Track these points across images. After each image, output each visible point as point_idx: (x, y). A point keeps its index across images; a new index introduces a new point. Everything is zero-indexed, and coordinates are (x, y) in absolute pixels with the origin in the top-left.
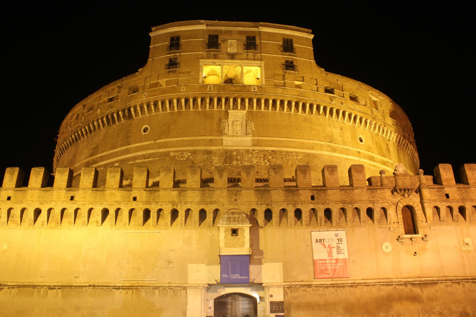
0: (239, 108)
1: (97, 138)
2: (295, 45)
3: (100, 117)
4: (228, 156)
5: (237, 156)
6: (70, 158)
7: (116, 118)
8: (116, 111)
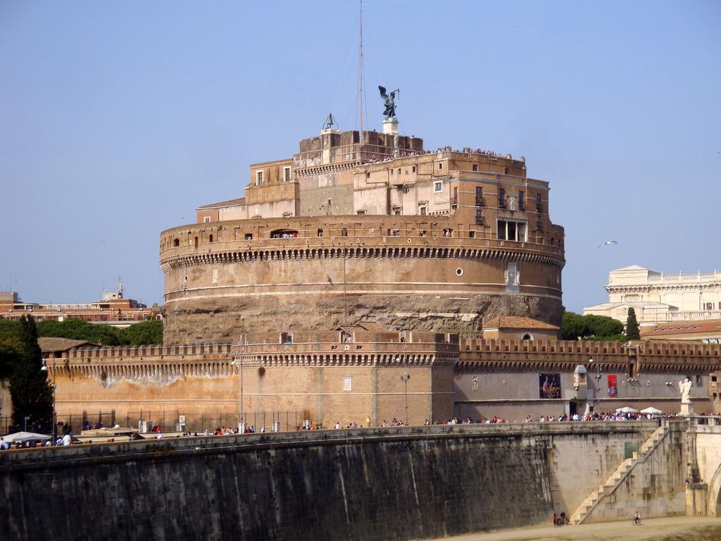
1: (405, 265)
2: (542, 200)
3: (413, 248)
4: (509, 301)
6: (361, 272)
8: (432, 248)
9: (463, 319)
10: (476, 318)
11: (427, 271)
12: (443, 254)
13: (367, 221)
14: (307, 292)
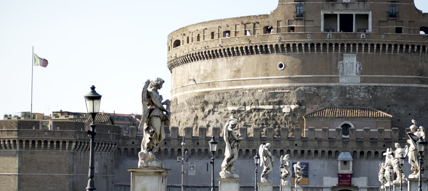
0: (351, 51)
1: (237, 63)
3: (239, 47)
4: (343, 91)
5: (349, 91)
6: (209, 71)
7: (254, 51)
8: (254, 45)
9: (284, 110)
10: (295, 109)
11: (253, 68)
12: (264, 50)
13: (210, 26)
14: (186, 92)
